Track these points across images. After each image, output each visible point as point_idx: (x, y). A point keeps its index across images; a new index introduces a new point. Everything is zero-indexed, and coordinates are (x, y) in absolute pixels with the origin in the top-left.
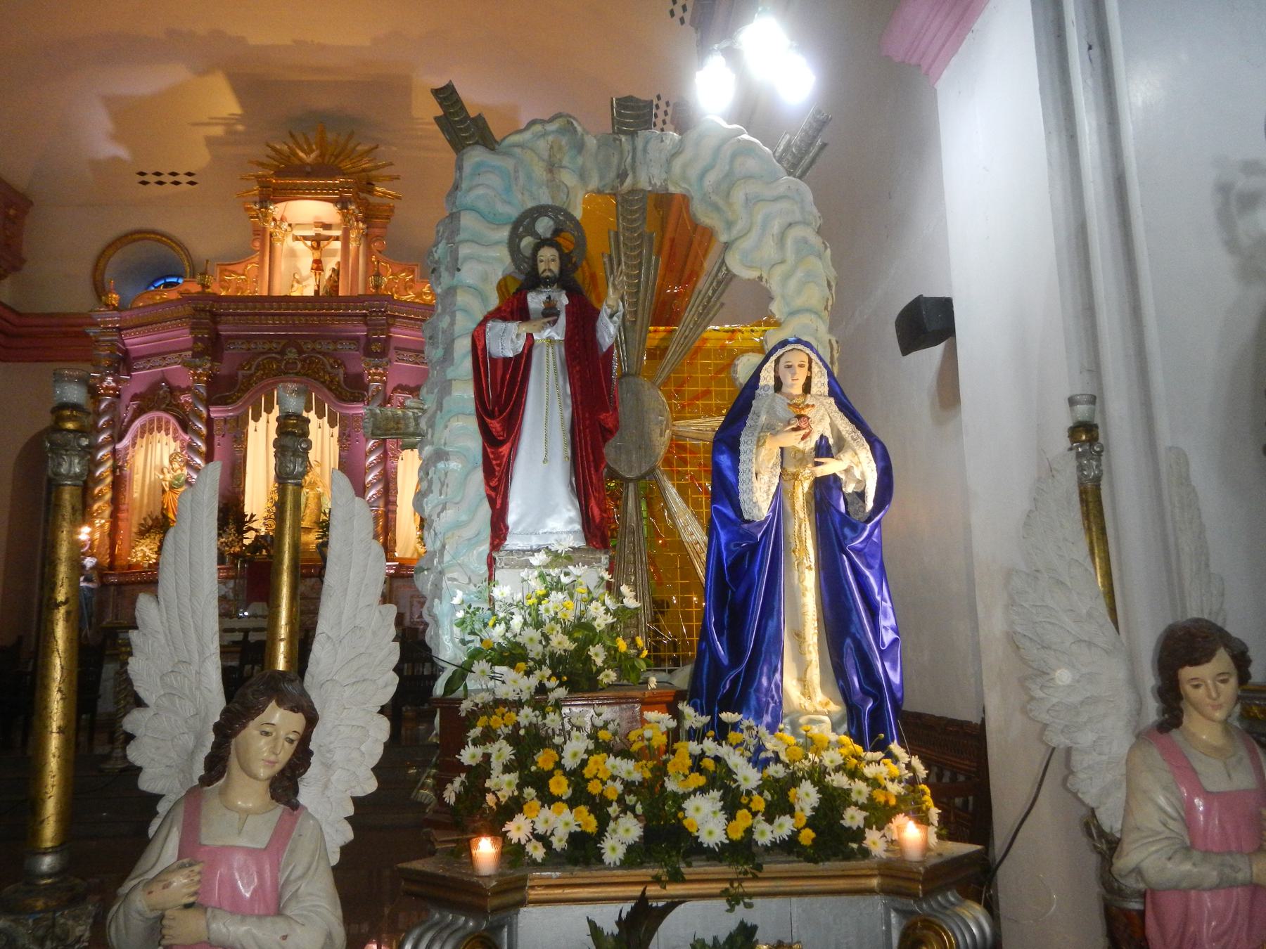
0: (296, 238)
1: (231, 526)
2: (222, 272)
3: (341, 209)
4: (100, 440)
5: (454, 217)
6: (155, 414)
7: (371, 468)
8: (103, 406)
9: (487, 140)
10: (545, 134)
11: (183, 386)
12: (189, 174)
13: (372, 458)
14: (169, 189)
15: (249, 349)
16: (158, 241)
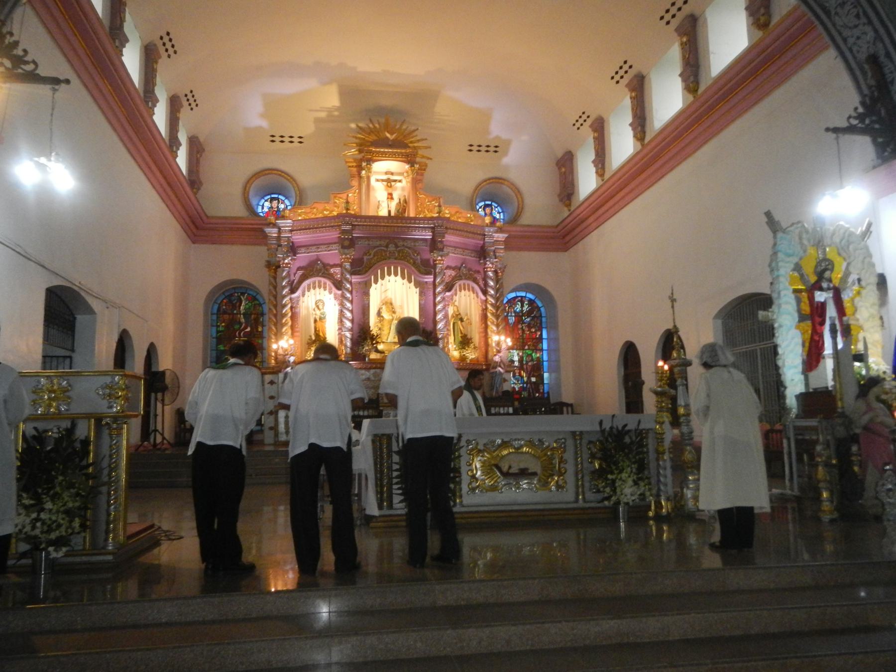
0: (377, 180)
1: (369, 341)
2: (335, 197)
3: (411, 167)
4: (284, 293)
5: (775, 254)
6: (317, 279)
7: (440, 311)
8: (284, 274)
9: (784, 231)
10: (797, 228)
11: (332, 263)
12: (300, 137)
13: (439, 307)
14: (287, 145)
15: (369, 244)
16: (280, 175)
